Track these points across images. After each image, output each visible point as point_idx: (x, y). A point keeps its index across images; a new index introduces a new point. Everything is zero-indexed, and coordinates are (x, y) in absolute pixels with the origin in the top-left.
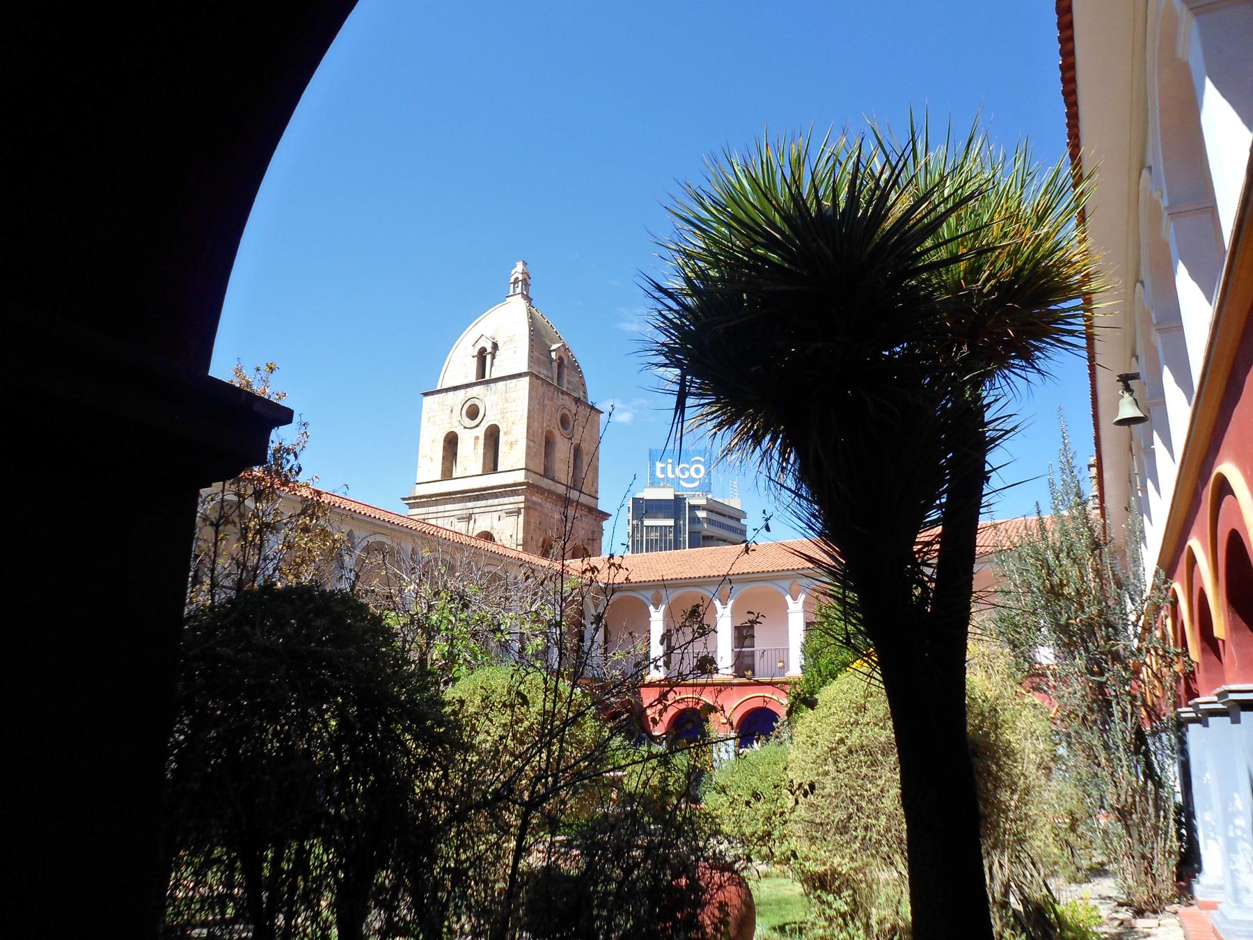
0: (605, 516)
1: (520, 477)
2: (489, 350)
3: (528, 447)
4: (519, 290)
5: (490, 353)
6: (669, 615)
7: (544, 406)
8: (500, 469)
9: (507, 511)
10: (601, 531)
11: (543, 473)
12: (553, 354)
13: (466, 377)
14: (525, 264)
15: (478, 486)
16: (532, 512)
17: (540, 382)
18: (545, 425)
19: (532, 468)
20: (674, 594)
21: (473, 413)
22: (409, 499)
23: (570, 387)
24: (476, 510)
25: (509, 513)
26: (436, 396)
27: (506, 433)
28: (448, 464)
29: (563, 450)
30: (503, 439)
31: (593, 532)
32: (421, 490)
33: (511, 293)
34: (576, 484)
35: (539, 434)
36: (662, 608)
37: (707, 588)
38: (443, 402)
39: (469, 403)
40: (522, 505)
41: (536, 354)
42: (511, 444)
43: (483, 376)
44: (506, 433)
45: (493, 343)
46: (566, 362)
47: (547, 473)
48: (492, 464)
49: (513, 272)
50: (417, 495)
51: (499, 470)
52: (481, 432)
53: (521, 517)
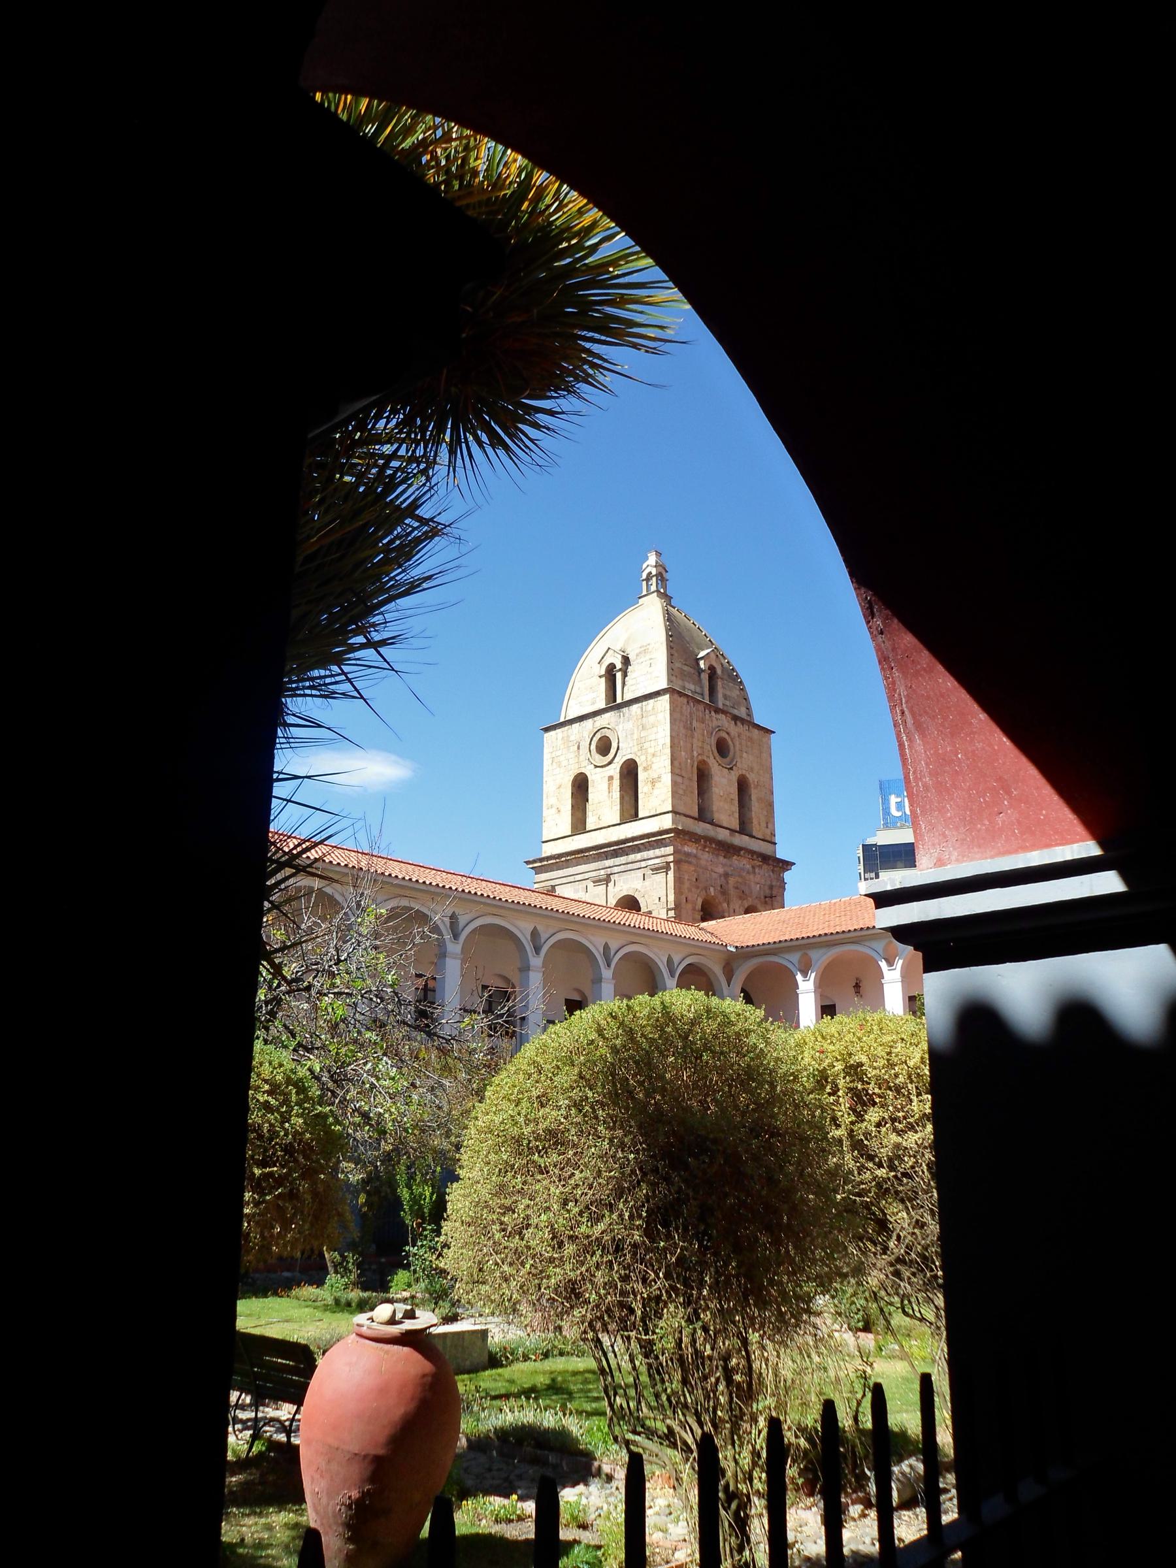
0: (786, 865)
1: (667, 822)
2: (619, 666)
3: (674, 784)
4: (653, 588)
5: (620, 670)
6: (821, 987)
7: (692, 730)
9: (653, 867)
10: (782, 885)
11: (696, 815)
12: (702, 664)
13: (593, 703)
14: (659, 554)
15: (614, 839)
16: (685, 867)
17: (685, 700)
18: (695, 754)
19: (681, 809)
20: (825, 957)
21: (604, 747)
22: (534, 861)
23: (728, 703)
24: (616, 869)
25: (656, 870)
26: (558, 731)
28: (579, 814)
29: (723, 784)
30: (642, 776)
31: (771, 887)
32: (549, 850)
33: (644, 592)
34: (744, 828)
38: (568, 736)
39: (598, 736)
40: (671, 858)
41: (678, 665)
42: (653, 782)
43: (615, 701)
44: (645, 769)
45: (623, 656)
46: (719, 671)
48: (630, 810)
49: (644, 566)
50: (544, 855)
51: (640, 816)
52: (615, 770)
53: (671, 874)
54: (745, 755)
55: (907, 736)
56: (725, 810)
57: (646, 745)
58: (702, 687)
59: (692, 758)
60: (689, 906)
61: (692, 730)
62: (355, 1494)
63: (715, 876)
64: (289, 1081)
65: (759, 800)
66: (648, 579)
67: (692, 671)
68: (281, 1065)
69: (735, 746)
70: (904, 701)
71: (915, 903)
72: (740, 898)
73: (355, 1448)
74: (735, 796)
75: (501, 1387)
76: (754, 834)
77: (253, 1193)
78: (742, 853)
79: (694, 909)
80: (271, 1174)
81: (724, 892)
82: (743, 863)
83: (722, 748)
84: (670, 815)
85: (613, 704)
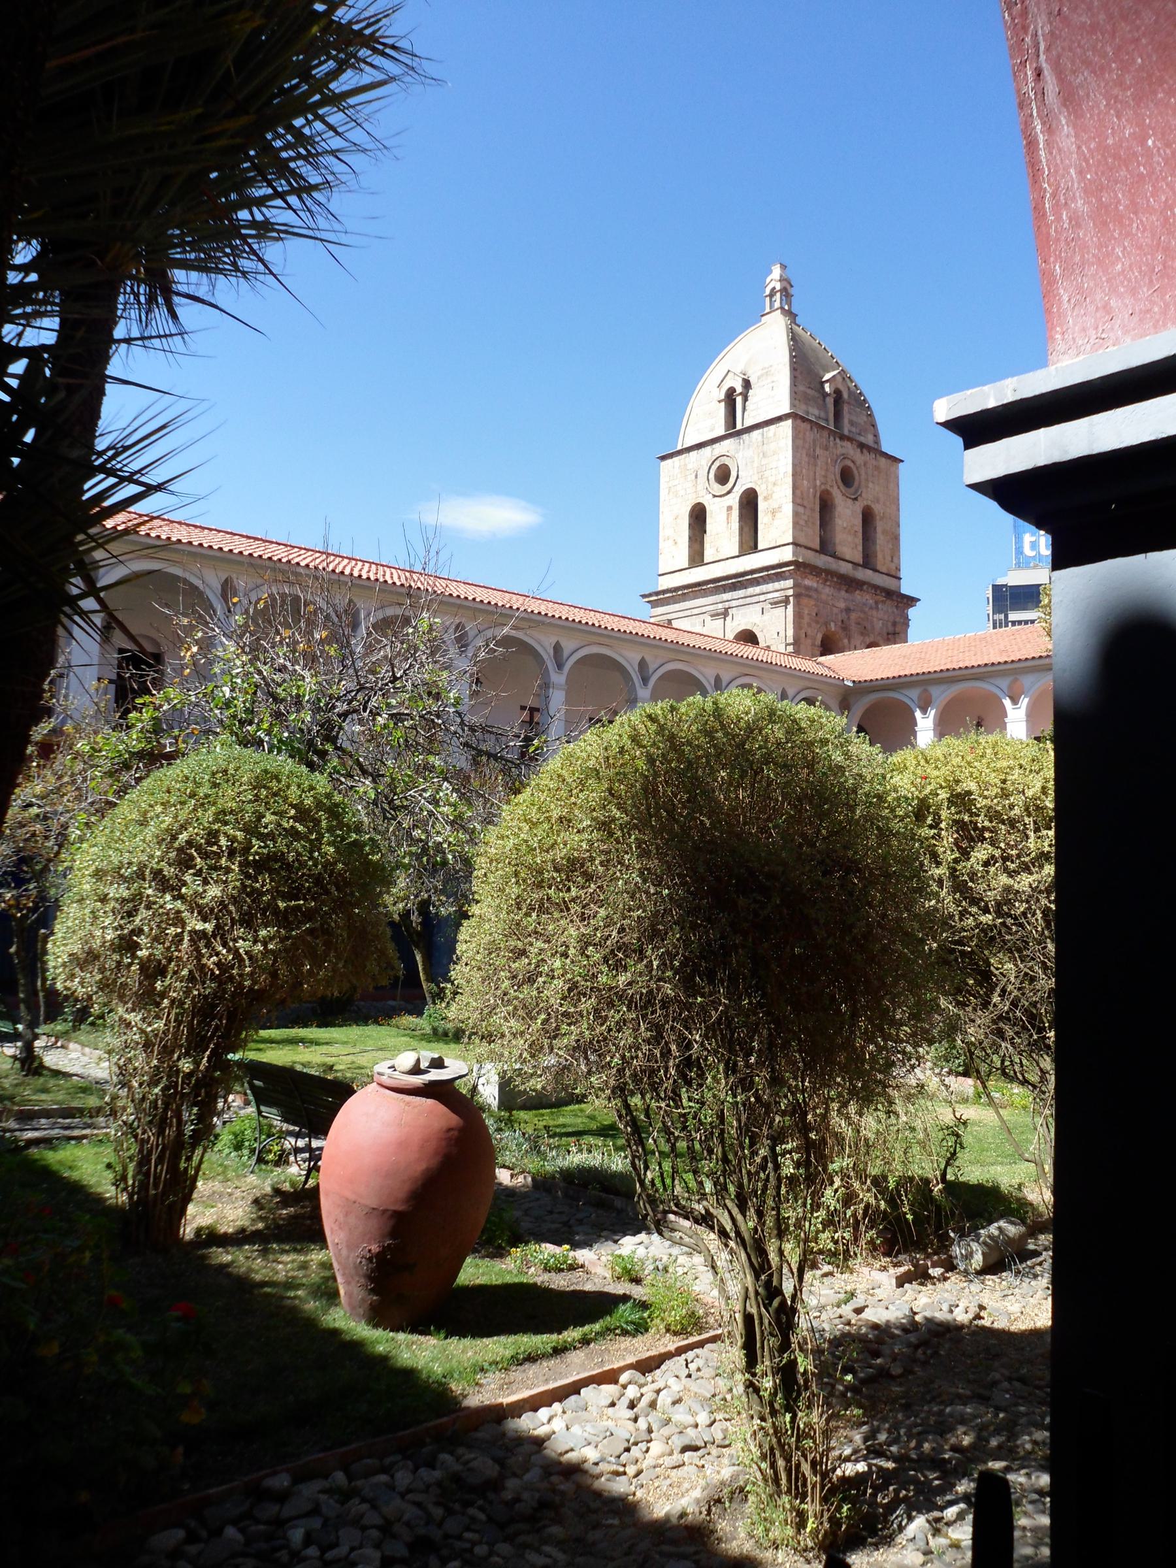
0: (911, 601)
1: (787, 554)
3: (796, 514)
4: (777, 305)
7: (816, 457)
10: (906, 622)
12: (827, 388)
13: (712, 430)
15: (732, 571)
16: (805, 601)
17: (807, 426)
18: (818, 483)
19: (802, 541)
21: (723, 475)
22: (650, 595)
23: (854, 429)
24: (734, 603)
25: (775, 604)
26: (675, 459)
27: (766, 499)
28: (697, 546)
29: (847, 515)
30: (762, 506)
31: (894, 624)
32: (666, 583)
33: (768, 310)
34: (868, 562)
35: (811, 495)
36: (932, 713)
37: (992, 681)
39: (717, 464)
40: (791, 592)
41: (801, 388)
42: (774, 513)
43: (735, 427)
44: (766, 499)
46: (845, 395)
47: (825, 547)
48: (750, 542)
49: (768, 280)
50: (660, 588)
51: (760, 548)
52: (734, 500)
53: (790, 608)
55: (1043, 124)
56: (848, 544)
57: (767, 474)
58: (827, 413)
59: (815, 487)
60: (809, 641)
61: (816, 457)
62: (375, 1248)
64: (319, 805)
65: (884, 532)
66: (772, 295)
67: (816, 394)
68: (312, 788)
69: (860, 476)
70: (1042, 47)
71: (1042, 430)
72: (862, 634)
73: (373, 1202)
74: (859, 528)
75: (579, 1123)
76: (879, 567)
77: (279, 928)
78: (865, 587)
79: (813, 645)
80: (299, 907)
81: (845, 628)
83: (847, 477)
85: (733, 430)
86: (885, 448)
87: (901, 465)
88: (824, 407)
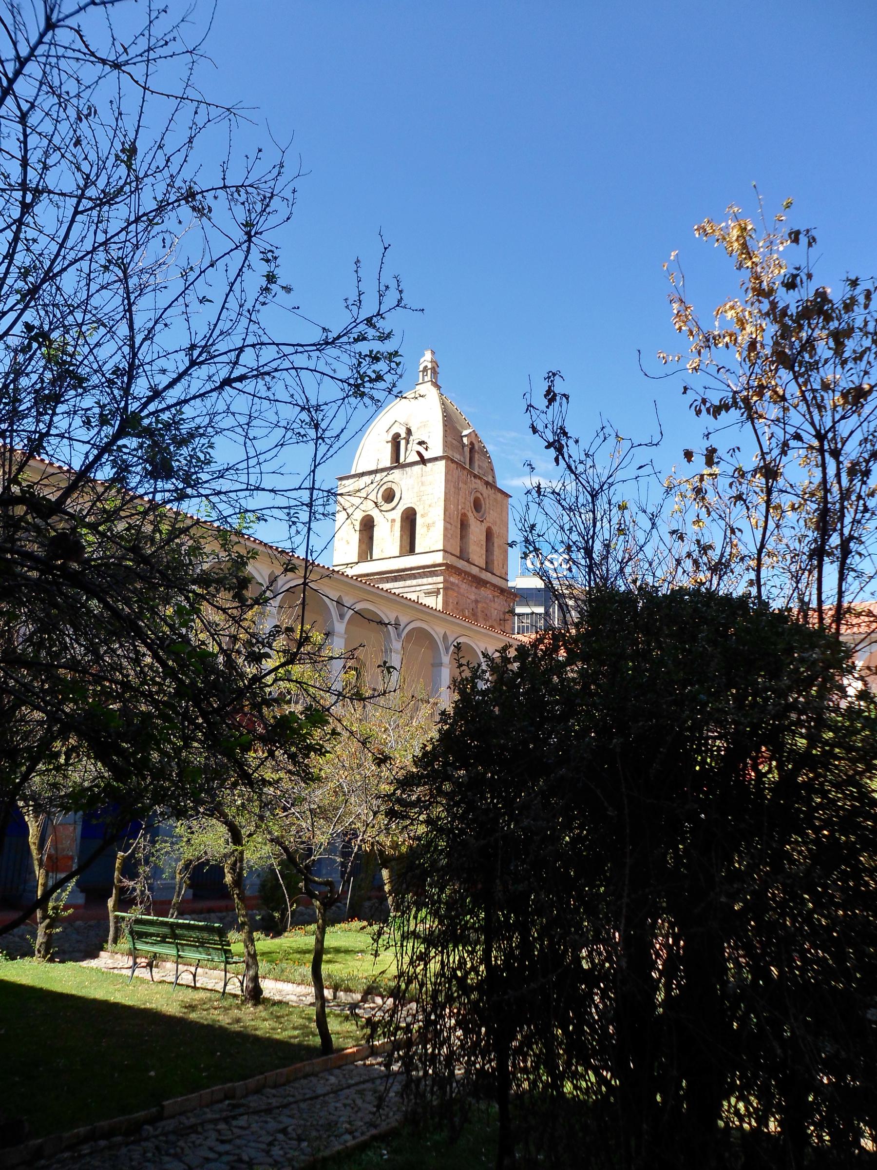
1: (438, 558)
2: (403, 435)
7: (459, 489)
8: (417, 551)
11: (458, 554)
12: (465, 440)
14: (433, 353)
15: (396, 568)
16: (450, 592)
17: (455, 466)
27: (422, 516)
29: (477, 531)
33: (421, 381)
34: (488, 569)
39: (385, 487)
40: (441, 586)
41: (449, 439)
42: (428, 527)
44: (422, 516)
46: (476, 447)
48: (409, 546)
49: (422, 360)
52: (397, 515)
53: (440, 597)
54: (491, 512)
56: (477, 554)
57: (424, 498)
61: (459, 489)
63: (469, 601)
65: (499, 546)
66: (425, 369)
69: (486, 505)
72: (485, 619)
82: (486, 593)
83: (477, 505)
84: (442, 553)
86: (499, 485)
87: (510, 499)
88: (462, 454)
